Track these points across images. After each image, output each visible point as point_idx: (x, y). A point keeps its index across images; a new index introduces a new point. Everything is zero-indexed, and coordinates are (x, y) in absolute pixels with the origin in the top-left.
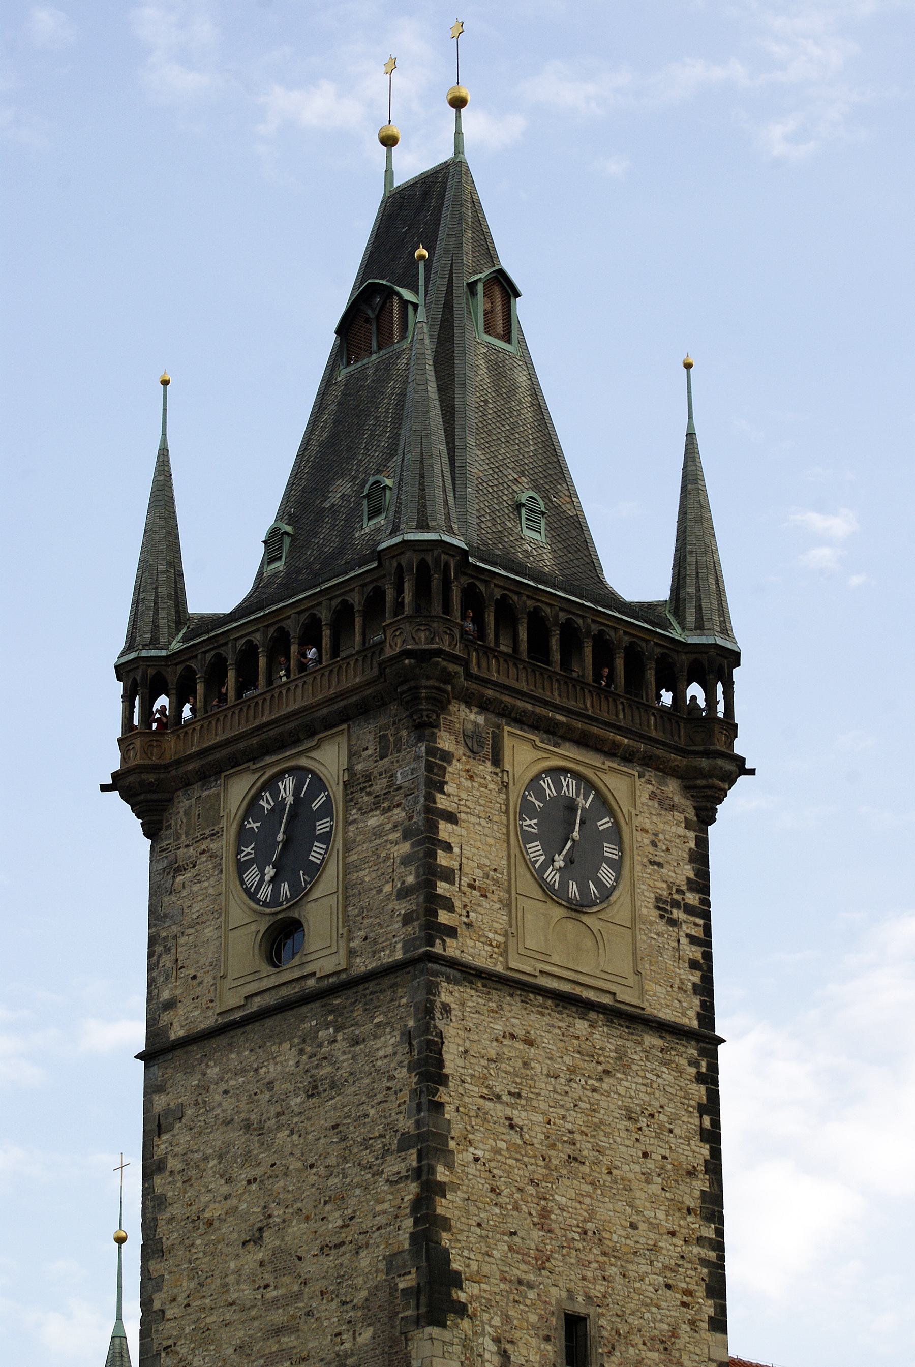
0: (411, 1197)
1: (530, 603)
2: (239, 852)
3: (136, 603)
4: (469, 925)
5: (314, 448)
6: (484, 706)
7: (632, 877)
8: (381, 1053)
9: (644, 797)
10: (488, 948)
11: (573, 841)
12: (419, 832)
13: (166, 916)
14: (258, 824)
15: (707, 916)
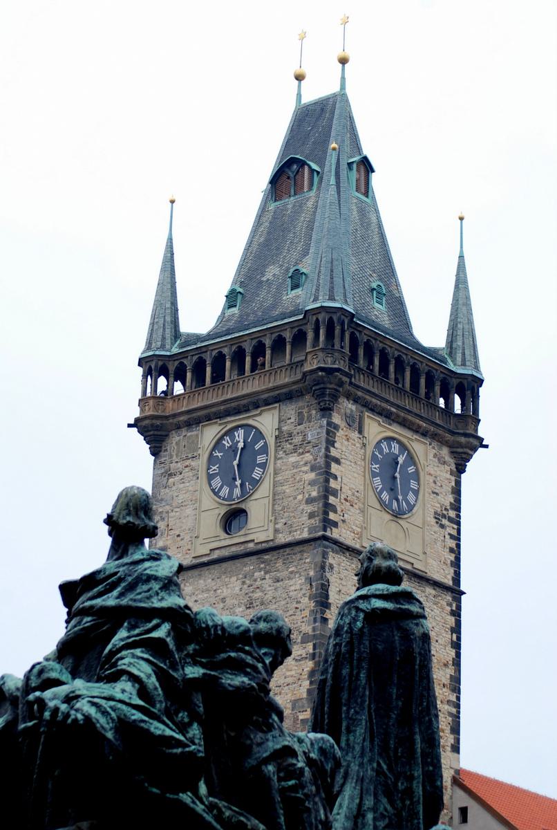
0: (309, 669)
1: (381, 345)
2: (209, 469)
3: (152, 324)
4: (344, 521)
5: (255, 246)
6: (356, 400)
7: (424, 500)
8: (293, 588)
9: (431, 456)
10: (352, 534)
11: (394, 478)
12: (320, 468)
13: (162, 500)
14: (222, 454)
15: (459, 524)
